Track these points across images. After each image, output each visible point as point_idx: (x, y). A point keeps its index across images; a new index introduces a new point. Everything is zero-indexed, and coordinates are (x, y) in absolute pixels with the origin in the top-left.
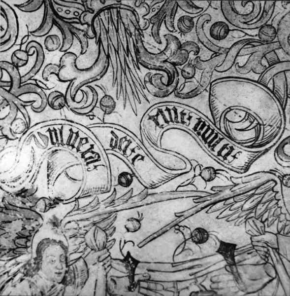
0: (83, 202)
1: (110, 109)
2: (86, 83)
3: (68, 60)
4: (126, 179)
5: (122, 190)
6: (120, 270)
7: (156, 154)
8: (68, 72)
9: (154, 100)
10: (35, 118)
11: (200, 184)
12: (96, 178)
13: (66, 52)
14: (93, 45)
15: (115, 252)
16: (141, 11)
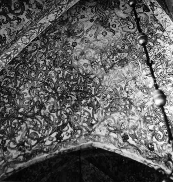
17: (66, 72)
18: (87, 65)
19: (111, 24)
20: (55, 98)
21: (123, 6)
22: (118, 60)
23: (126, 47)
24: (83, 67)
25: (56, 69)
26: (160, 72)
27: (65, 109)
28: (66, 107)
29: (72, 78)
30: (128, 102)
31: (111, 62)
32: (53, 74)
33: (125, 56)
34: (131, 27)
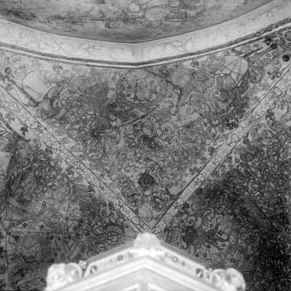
0: (66, 227)
1: (87, 234)
2: (93, 230)
3: (98, 227)
4: (69, 237)
5: (67, 236)
6: (51, 235)
7: (75, 245)
8: (96, 226)
9: (87, 245)
10: (86, 218)
11: (67, 255)
12: (71, 230)
13: (100, 227)
14: (101, 233)
15: (54, 234)
16: (107, 244)
17: (258, 269)
18: (252, 247)
19: (210, 229)
20: (278, 283)
21: (190, 223)
22: (244, 217)
23: (230, 211)
24: (255, 250)
25: (254, 280)
26: (240, 181)
27: (288, 272)
28: (286, 271)
29: (263, 263)
30: (277, 206)
31: (247, 224)
32: (258, 283)
33: (239, 212)
34: (209, 212)
